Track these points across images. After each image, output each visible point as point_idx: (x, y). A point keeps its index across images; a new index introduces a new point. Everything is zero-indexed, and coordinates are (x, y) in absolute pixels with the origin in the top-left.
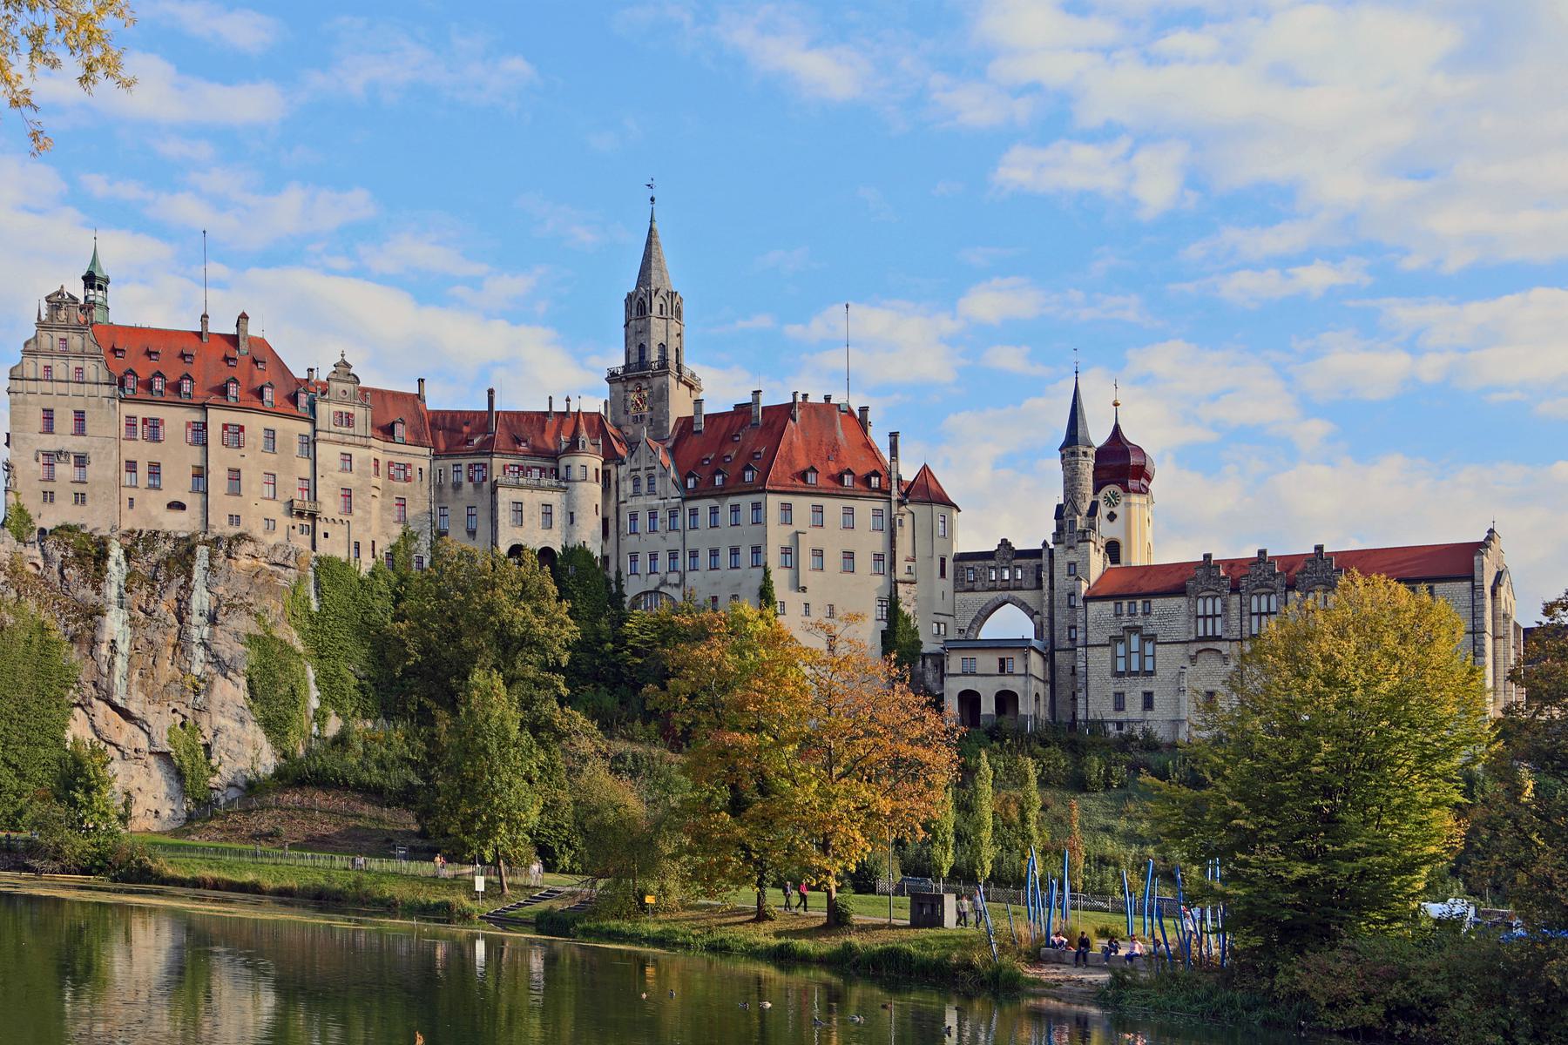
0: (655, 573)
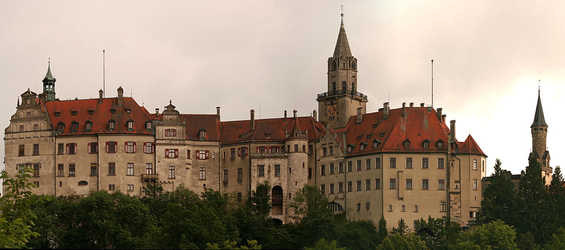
0: (333, 193)
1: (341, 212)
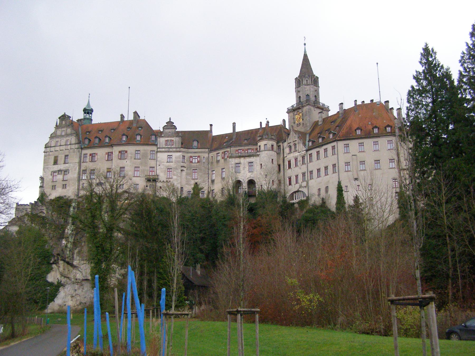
0: (298, 183)
1: (305, 198)
